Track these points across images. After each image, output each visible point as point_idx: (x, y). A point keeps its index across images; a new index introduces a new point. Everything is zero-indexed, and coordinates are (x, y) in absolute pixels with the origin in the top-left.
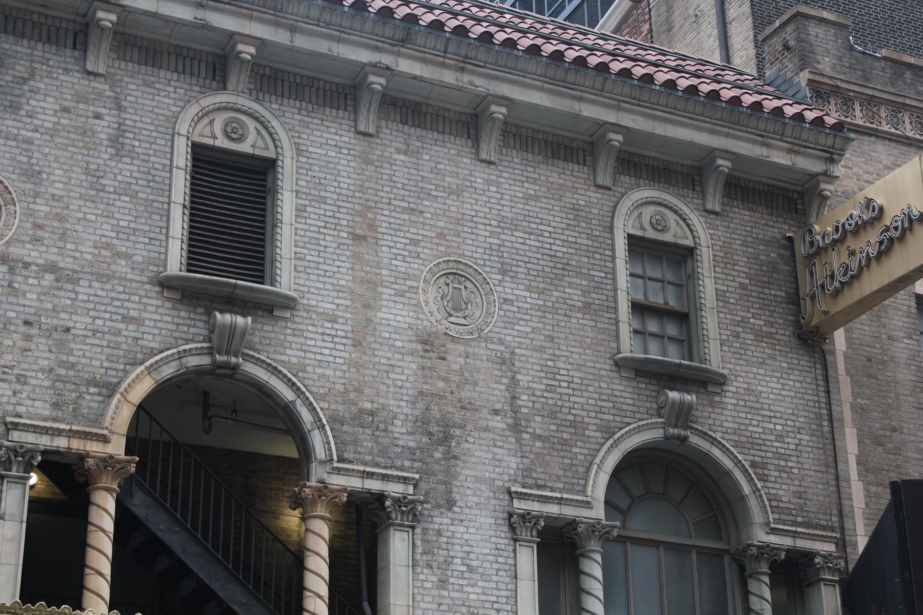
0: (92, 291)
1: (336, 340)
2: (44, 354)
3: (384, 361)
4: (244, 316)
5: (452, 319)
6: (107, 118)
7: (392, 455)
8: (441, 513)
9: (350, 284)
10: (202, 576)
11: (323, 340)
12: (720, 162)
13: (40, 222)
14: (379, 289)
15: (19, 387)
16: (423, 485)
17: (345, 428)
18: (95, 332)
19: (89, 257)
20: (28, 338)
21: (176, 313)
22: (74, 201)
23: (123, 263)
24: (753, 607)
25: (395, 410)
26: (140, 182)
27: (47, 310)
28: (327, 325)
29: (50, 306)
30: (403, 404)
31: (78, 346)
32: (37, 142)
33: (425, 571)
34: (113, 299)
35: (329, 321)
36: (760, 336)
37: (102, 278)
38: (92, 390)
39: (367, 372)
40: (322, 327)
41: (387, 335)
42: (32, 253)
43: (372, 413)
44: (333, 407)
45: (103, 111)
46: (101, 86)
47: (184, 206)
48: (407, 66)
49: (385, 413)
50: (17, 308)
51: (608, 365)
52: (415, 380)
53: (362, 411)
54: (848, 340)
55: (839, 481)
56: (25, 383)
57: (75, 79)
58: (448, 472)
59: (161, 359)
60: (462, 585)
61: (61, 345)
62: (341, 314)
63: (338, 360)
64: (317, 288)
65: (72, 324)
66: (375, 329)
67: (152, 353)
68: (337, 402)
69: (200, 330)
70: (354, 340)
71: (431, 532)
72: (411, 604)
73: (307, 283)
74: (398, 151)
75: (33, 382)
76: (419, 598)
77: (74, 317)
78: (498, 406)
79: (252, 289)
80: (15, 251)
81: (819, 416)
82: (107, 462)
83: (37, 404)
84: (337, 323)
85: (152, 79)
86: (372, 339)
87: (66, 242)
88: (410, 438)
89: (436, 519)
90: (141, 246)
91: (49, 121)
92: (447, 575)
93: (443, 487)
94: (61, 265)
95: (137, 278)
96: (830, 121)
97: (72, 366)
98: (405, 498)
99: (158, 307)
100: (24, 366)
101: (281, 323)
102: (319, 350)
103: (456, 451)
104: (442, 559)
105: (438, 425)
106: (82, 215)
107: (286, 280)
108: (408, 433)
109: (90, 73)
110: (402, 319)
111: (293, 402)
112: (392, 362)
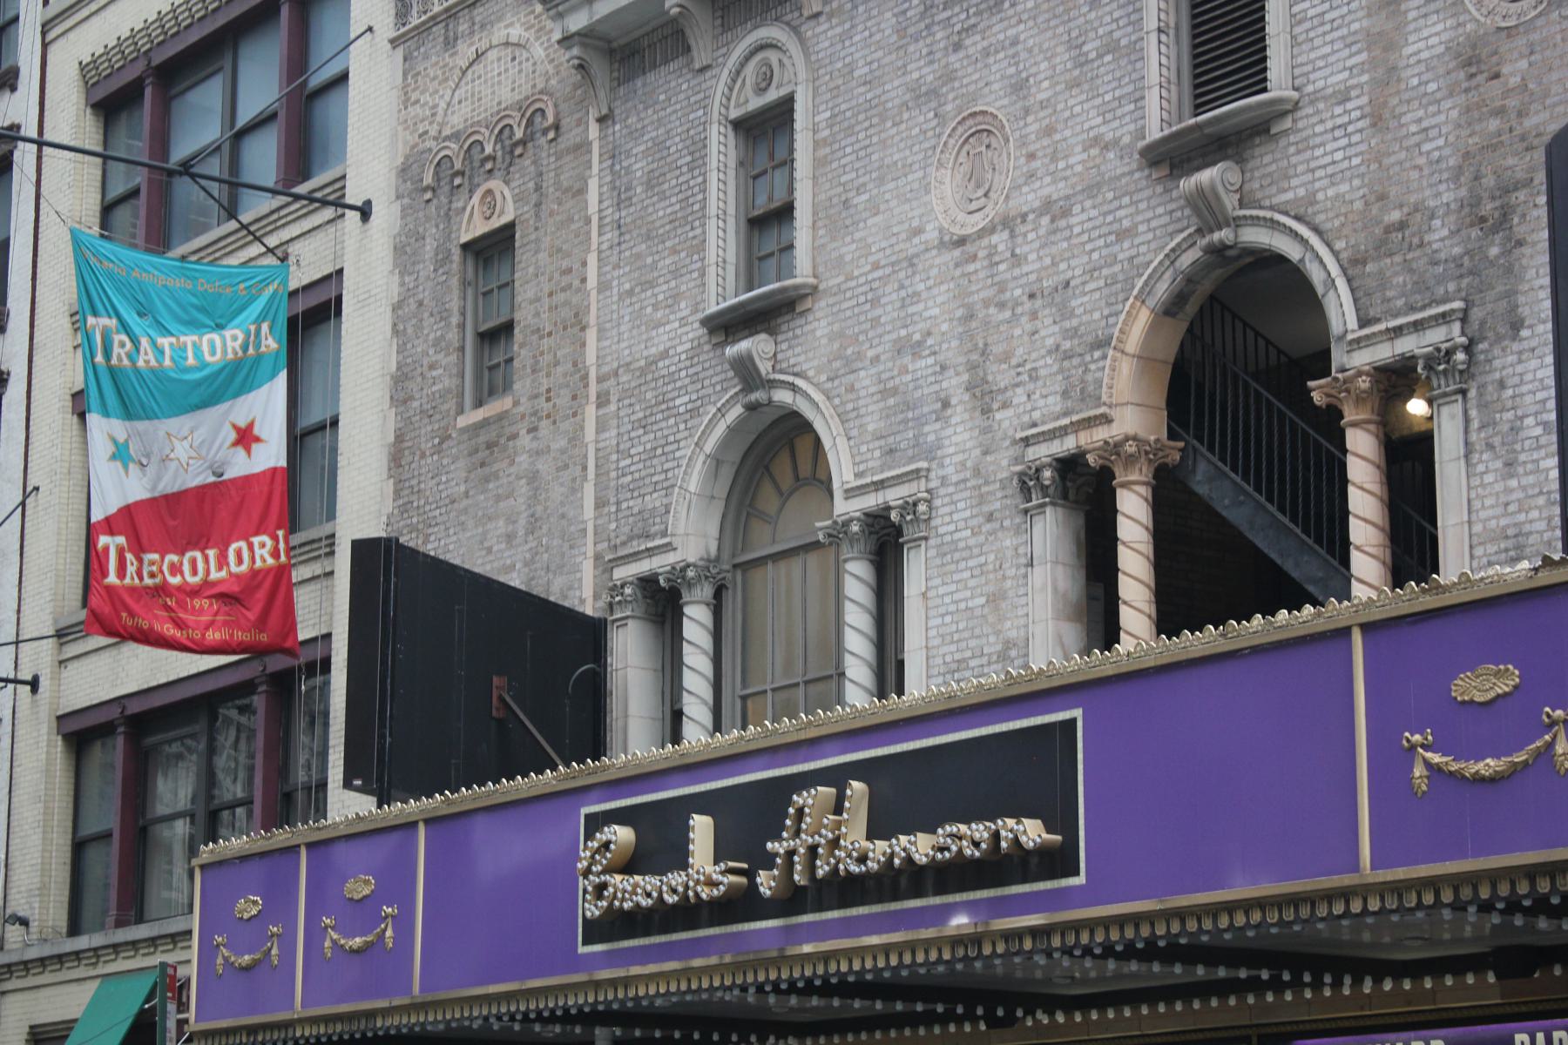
0: (1084, 217)
1: (1350, 129)
2: (1050, 333)
3: (1413, 128)
4: (1214, 163)
7: (1432, 282)
8: (1503, 350)
9: (1365, 23)
10: (1273, 556)
11: (1335, 139)
13: (1032, 148)
14: (1403, 7)
15: (1032, 386)
16: (1476, 314)
17: (1368, 268)
19: (1079, 168)
20: (1034, 316)
21: (1167, 197)
22: (1060, 98)
23: (1111, 155)
25: (1432, 203)
26: (1121, 23)
27: (1046, 268)
28: (1338, 110)
30: (1443, 187)
31: (1079, 301)
32: (1022, 37)
33: (1485, 457)
34: (1105, 214)
35: (1339, 103)
37: (1092, 190)
38: (1097, 354)
39: (1393, 159)
40: (1333, 117)
41: (1415, 81)
42: (1030, 197)
43: (1402, 226)
44: (1353, 242)
47: (1160, 30)
49: (1418, 216)
50: (1023, 281)
52: (1458, 137)
56: (1037, 378)
58: (1509, 270)
59: (1150, 277)
60: (1537, 461)
61: (1065, 312)
62: (1354, 81)
63: (1356, 161)
64: (1324, 57)
65: (1070, 274)
66: (1399, 80)
68: (1355, 230)
70: (1372, 115)
71: (1490, 388)
72: (1466, 518)
73: (1313, 56)
76: (1477, 504)
77: (1073, 263)
79: (1217, 119)
82: (1114, 448)
83: (1051, 400)
84: (1349, 99)
86: (1395, 101)
87: (1057, 160)
88: (1456, 240)
89: (1497, 363)
90: (1127, 119)
92: (1515, 451)
93: (1504, 303)
94: (1055, 197)
95: (1126, 169)
97: (1076, 329)
98: (1438, 350)
99: (1149, 199)
100: (1034, 355)
101: (1283, 142)
102: (1328, 159)
103: (1520, 230)
104: (1506, 427)
105: (1493, 198)
106: (1067, 114)
108: (1452, 233)
110: (1434, 40)
111: (1302, 260)
112: (1425, 124)
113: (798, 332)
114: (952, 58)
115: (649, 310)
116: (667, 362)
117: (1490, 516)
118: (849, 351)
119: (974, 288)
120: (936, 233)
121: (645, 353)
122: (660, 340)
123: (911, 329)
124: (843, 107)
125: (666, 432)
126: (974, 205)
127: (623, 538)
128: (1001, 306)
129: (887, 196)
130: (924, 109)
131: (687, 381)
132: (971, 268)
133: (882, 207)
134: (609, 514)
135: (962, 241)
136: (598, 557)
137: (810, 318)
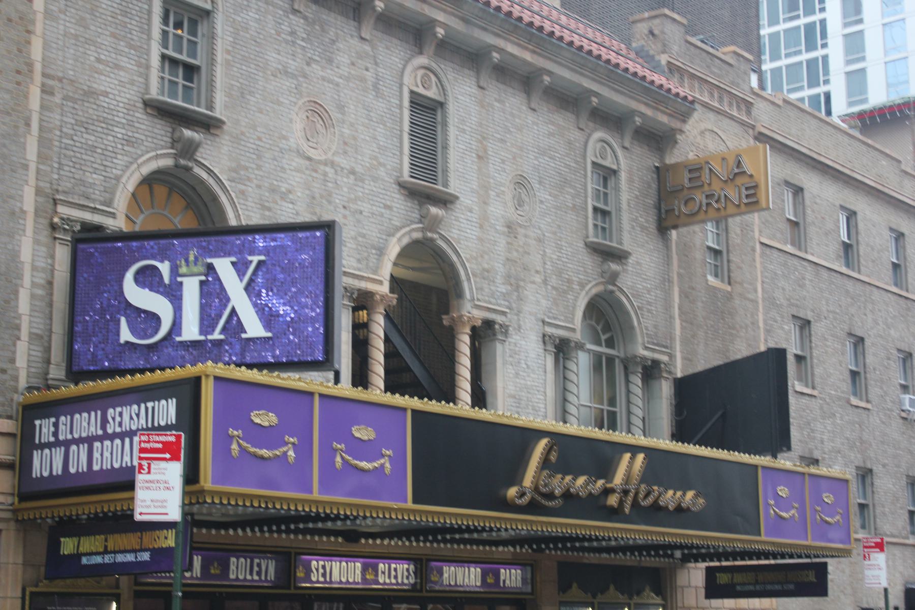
0: (369, 187)
5: (519, 212)
6: (371, 70)
12: (637, 119)
13: (346, 140)
18: (373, 214)
19: (368, 165)
21: (405, 203)
24: (631, 390)
28: (469, 214)
29: (353, 196)
36: (643, 228)
37: (375, 179)
38: (374, 251)
43: (488, 271)
45: (369, 65)
46: (367, 48)
48: (511, 48)
51: (581, 244)
53: (484, 270)
54: (678, 234)
55: (672, 317)
57: (355, 42)
65: (362, 209)
67: (398, 229)
69: (416, 215)
74: (496, 100)
75: (348, 245)
77: (364, 205)
78: (538, 268)
80: (337, 159)
81: (664, 278)
83: (351, 259)
85: (389, 44)
91: (345, 70)
93: (516, 317)
94: (357, 170)
96: (690, 98)
107: (454, 186)
109: (362, 38)
113: (209, 142)
114: (306, 67)
115: (92, 58)
116: (107, 100)
117: (511, 389)
118: (242, 173)
119: (315, 185)
120: (295, 146)
121: (88, 83)
122: (103, 83)
123: (280, 184)
124: (241, 43)
125: (106, 142)
126: (311, 144)
127: (66, 189)
128: (330, 202)
129: (268, 108)
130: (290, 80)
131: (124, 121)
132: (314, 175)
133: (265, 112)
134: (52, 167)
135: (309, 159)
136: (39, 192)
137: (217, 140)
